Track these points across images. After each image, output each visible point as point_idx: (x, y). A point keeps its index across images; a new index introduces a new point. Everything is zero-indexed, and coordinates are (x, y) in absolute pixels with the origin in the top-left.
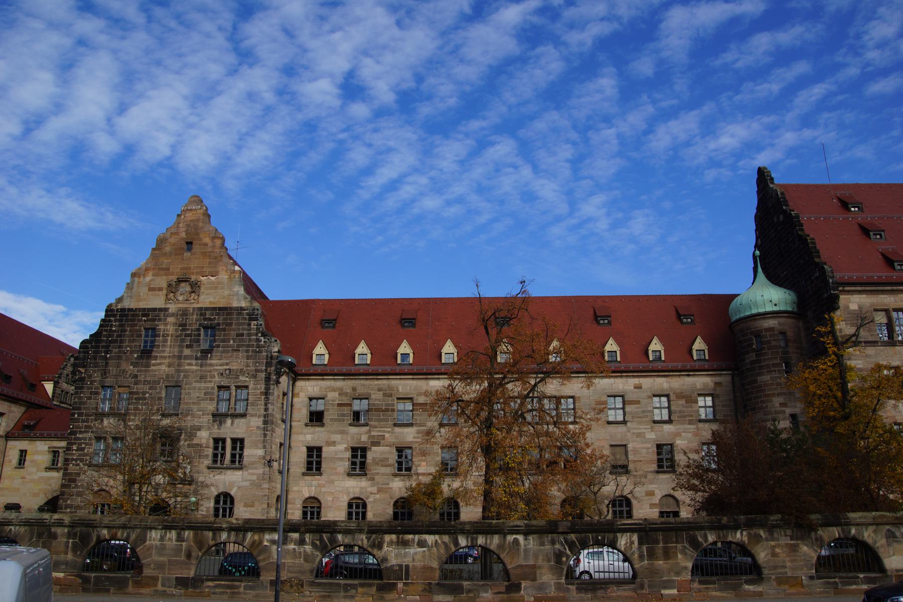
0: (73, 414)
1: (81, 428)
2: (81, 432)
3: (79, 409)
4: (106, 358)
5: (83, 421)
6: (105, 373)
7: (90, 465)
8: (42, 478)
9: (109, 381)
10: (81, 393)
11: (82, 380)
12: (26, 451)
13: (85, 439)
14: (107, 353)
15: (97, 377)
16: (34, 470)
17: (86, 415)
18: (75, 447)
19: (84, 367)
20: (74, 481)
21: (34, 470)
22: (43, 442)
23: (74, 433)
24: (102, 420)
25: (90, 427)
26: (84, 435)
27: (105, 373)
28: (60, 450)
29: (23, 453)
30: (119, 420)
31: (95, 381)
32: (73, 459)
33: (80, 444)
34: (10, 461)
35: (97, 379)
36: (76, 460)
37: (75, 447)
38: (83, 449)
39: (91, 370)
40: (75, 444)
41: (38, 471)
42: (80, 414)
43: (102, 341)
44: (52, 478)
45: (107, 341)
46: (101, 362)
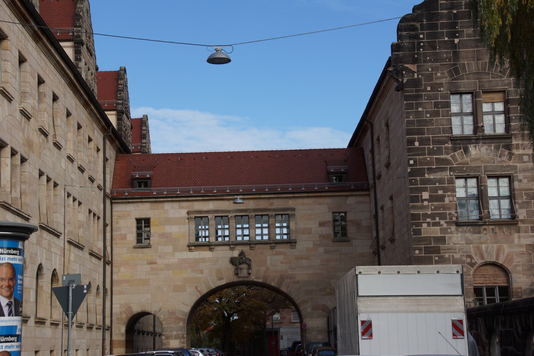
0: (411, 142)
1: (430, 163)
2: (430, 171)
3: (420, 132)
4: (454, 46)
5: (431, 152)
6: (455, 71)
7: (458, 224)
8: (185, 261)
9: (465, 83)
10: (418, 105)
11: (416, 83)
12: (147, 221)
13: (441, 181)
14: (453, 35)
15: (442, 77)
16: (170, 249)
17: (435, 142)
18: (426, 195)
19: (415, 61)
20: (437, 250)
21: (170, 249)
22: (176, 205)
23: (421, 173)
24: (466, 151)
25: (447, 161)
26: (438, 176)
27: (456, 71)
28: (210, 216)
29: (143, 224)
30: (497, 148)
32: (426, 216)
33: (436, 190)
34: (124, 237)
35: (444, 81)
36: (433, 216)
37: (426, 195)
38: (441, 198)
39: (429, 67)
40: (425, 190)
41: (175, 250)
42: (422, 142)
43: (441, 16)
44: (203, 260)
45: (449, 16)
46: (445, 53)
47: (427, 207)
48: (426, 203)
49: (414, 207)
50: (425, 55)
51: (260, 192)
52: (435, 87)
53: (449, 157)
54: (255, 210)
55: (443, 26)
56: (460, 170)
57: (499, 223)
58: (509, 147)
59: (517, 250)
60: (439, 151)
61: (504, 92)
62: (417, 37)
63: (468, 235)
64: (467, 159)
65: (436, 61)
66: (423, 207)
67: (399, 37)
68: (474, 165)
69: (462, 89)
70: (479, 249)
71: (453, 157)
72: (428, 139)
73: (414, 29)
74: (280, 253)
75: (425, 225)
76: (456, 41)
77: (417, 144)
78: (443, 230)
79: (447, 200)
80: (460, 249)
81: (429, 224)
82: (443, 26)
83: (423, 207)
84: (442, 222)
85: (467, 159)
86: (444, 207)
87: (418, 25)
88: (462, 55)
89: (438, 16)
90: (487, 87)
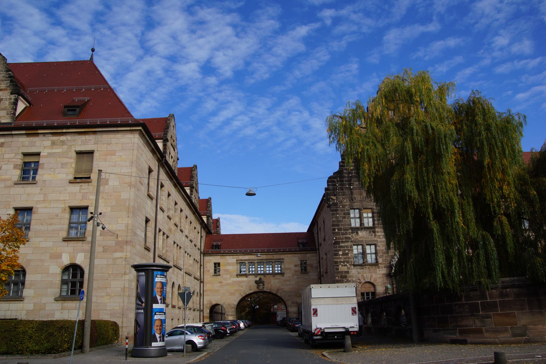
0: (334, 230)
1: (342, 239)
2: (343, 242)
3: (338, 225)
4: (351, 189)
5: (343, 234)
6: (352, 200)
7: (355, 265)
8: (234, 282)
9: (356, 205)
10: (337, 214)
11: (336, 204)
12: (219, 264)
13: (347, 247)
14: (350, 185)
15: (346, 202)
16: (228, 276)
17: (344, 230)
18: (341, 253)
19: (335, 195)
20: (346, 277)
21: (228, 276)
22: (231, 257)
24: (357, 233)
25: (349, 238)
26: (346, 244)
27: (353, 200)
28: (246, 262)
30: (370, 232)
31: (346, 205)
32: (341, 262)
33: (345, 250)
34: (209, 271)
35: (347, 204)
36: (344, 262)
37: (341, 253)
38: (347, 254)
40: (340, 250)
41: (231, 277)
42: (339, 229)
44: (243, 282)
45: (348, 177)
46: (347, 192)
47: (341, 258)
48: (341, 256)
49: (336, 258)
50: (339, 193)
51: (268, 251)
52: (344, 206)
53: (350, 236)
54: (266, 259)
55: (346, 181)
56: (355, 242)
57: (371, 265)
58: (374, 232)
59: (379, 276)
60: (346, 234)
61: (371, 209)
62: (335, 185)
63: (359, 270)
64: (358, 237)
65: (343, 195)
66: (340, 258)
67: (328, 185)
68: (361, 239)
69: (355, 207)
70: (363, 276)
71: (352, 236)
72: (341, 228)
73: (334, 182)
74: (277, 279)
75: (340, 266)
76: (352, 187)
77: (337, 230)
78: (348, 268)
79: (350, 255)
80: (355, 276)
81: (342, 265)
82: (346, 181)
83: (340, 258)
84: (348, 264)
85: (358, 237)
86: (349, 258)
87: (336, 180)
88: (354, 193)
89: (344, 177)
90: (365, 206)
